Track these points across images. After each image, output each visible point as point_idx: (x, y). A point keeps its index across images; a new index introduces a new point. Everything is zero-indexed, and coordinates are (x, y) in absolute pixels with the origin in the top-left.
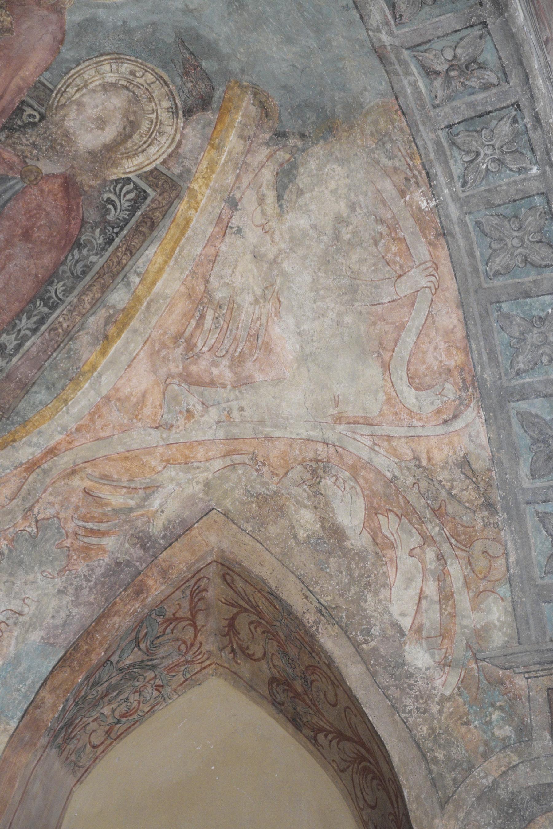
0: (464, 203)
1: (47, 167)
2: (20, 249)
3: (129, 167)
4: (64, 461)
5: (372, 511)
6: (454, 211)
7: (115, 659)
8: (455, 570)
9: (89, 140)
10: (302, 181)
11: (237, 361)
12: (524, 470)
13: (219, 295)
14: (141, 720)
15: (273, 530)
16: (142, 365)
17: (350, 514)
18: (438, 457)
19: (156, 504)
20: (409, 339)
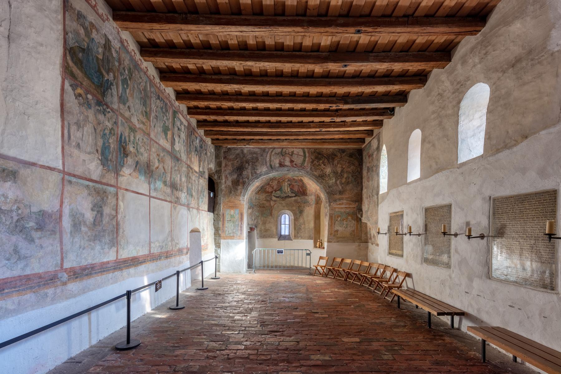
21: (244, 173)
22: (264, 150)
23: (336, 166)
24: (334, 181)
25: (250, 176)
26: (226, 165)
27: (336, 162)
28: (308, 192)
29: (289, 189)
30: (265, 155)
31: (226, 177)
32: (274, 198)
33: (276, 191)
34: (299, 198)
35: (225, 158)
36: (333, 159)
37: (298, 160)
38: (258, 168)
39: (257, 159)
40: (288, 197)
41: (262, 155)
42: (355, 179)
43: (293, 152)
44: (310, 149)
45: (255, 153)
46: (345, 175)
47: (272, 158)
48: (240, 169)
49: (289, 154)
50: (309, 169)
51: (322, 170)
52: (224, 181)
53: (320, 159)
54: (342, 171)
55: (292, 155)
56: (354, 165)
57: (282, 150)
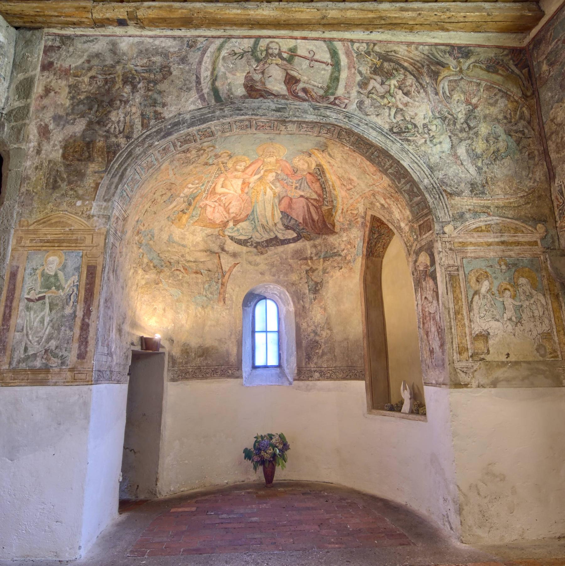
0: (351, 145)
1: (305, 173)
2: (314, 185)
3: (313, 166)
4: (345, 210)
5: (385, 199)
6: (351, 147)
7: (371, 238)
8: (399, 206)
9: (305, 167)
10: (332, 155)
11: (351, 184)
12: (397, 183)
13: (340, 176)
14: (389, 243)
15: (375, 208)
16: (342, 191)
17: (383, 202)
18: (385, 185)
19: (360, 211)
20: (366, 168)
21: (113, 116)
22: (192, 44)
23: (448, 98)
24: (446, 146)
25: (138, 126)
26: (47, 91)
27: (444, 85)
28: (338, 218)
29: (278, 215)
30: (194, 57)
31: (44, 132)
32: (231, 246)
33: (236, 222)
34: (308, 244)
35: (47, 67)
36: (435, 75)
37: (315, 78)
38: (168, 100)
39: (166, 72)
40: (275, 242)
41: (183, 60)
42: (518, 142)
43: (293, 52)
44: (352, 41)
45: (157, 52)
46: (484, 129)
47: (221, 69)
48: (99, 103)
49: (280, 55)
50: (353, 107)
51: (399, 110)
52: (33, 144)
53: (389, 75)
54: (470, 115)
55: (290, 60)
56: (506, 95)
57: (256, 44)
